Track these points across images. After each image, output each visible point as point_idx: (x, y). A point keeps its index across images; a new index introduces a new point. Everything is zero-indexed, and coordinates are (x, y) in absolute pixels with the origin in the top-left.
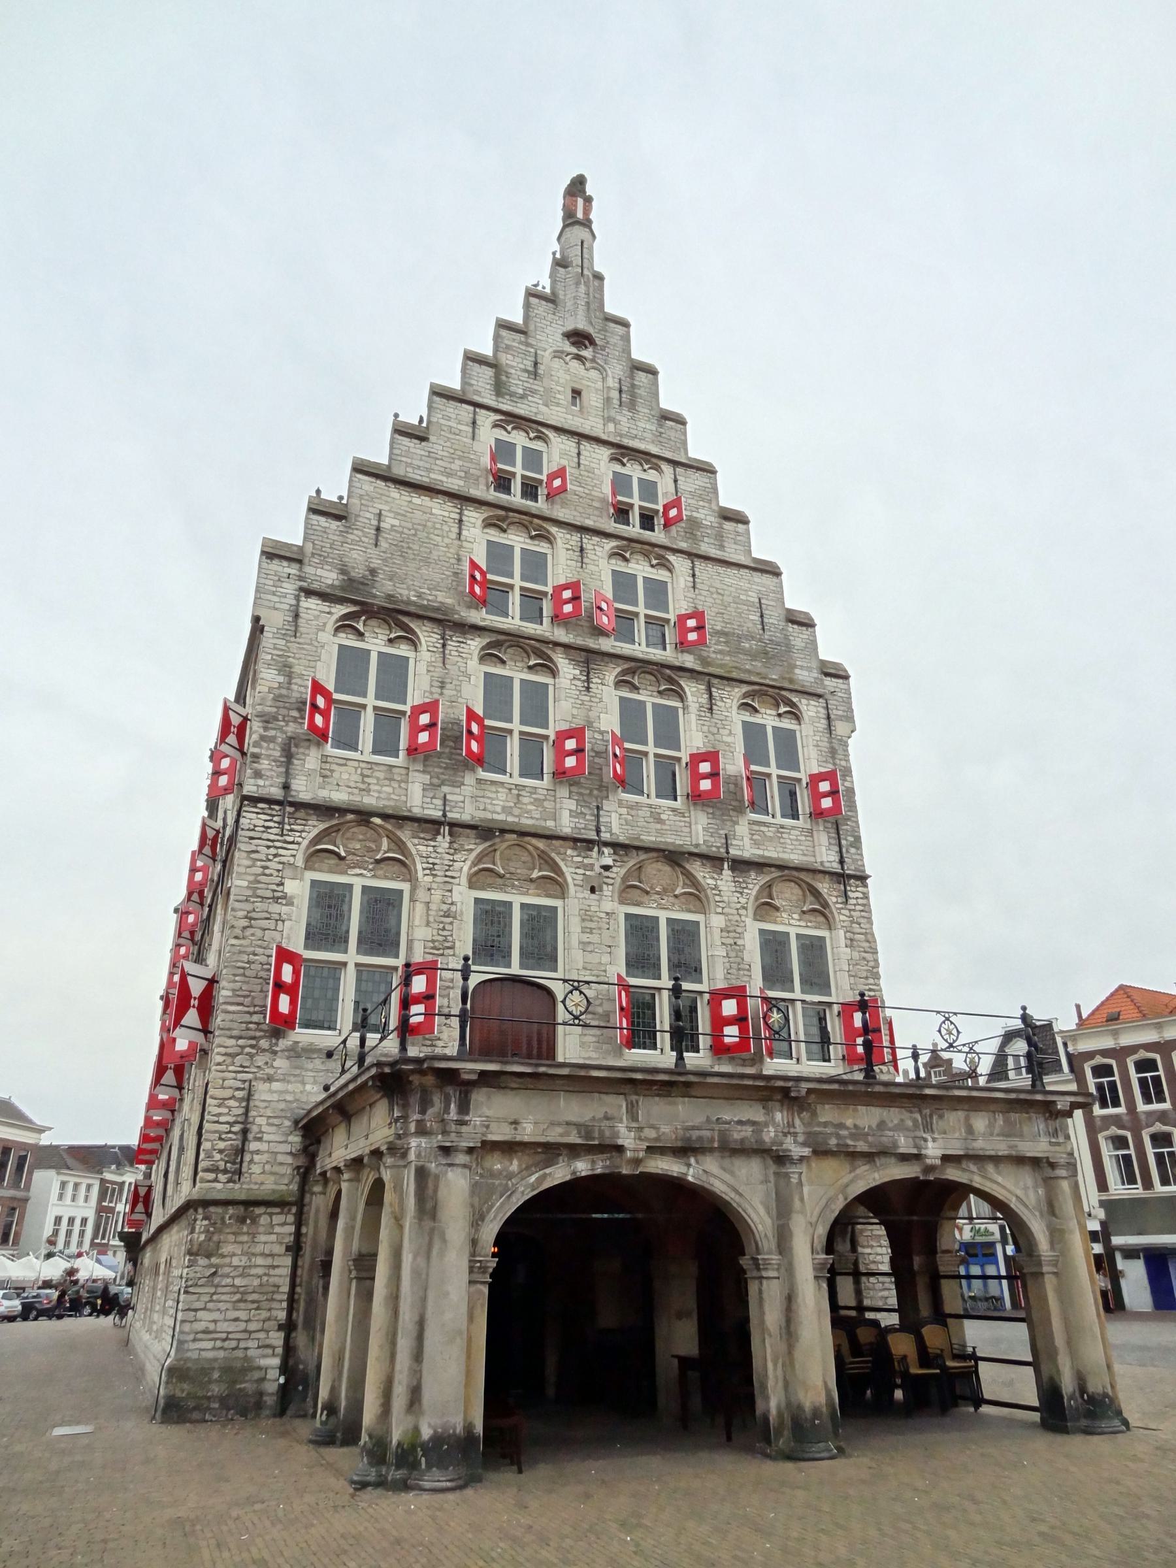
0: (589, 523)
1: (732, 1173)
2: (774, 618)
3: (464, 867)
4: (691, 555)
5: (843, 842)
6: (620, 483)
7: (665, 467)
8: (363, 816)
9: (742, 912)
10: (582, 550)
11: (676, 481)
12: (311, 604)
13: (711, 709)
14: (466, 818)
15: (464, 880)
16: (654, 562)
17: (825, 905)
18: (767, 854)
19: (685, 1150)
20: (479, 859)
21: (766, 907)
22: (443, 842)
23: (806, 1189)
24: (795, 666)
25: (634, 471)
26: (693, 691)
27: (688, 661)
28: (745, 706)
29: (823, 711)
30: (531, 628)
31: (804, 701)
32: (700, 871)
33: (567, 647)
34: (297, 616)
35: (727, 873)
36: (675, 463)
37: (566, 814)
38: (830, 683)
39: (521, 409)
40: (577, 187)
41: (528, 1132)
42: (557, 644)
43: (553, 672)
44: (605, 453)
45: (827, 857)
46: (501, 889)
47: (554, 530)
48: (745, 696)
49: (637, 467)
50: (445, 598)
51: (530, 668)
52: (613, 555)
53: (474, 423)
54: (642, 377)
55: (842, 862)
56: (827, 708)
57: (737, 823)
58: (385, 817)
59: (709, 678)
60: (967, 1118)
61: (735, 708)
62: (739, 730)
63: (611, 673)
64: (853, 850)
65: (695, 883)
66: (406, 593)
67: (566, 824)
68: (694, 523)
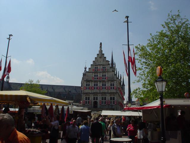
4: (108, 72)
6: (103, 68)
8: (88, 93)
12: (85, 82)
25: (104, 66)
30: (97, 80)
32: (106, 94)
36: (107, 65)
40: (101, 44)
43: (98, 83)
44: (102, 66)
50: (92, 79)
54: (105, 59)
59: (108, 81)
62: (110, 84)
66: (89, 80)
67: (98, 92)
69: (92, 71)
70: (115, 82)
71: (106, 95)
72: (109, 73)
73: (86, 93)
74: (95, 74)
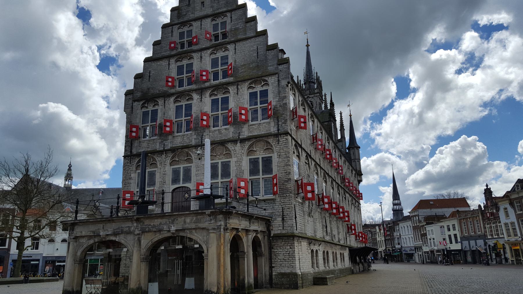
0: (204, 47)
1: (126, 239)
2: (262, 51)
3: (168, 161)
4: (235, 42)
5: (280, 123)
6: (215, 27)
7: (229, 14)
9: (243, 155)
10: (201, 57)
11: (231, 18)
12: (136, 104)
13: (238, 93)
14: (169, 148)
15: (168, 164)
16: (224, 50)
17: (272, 146)
18: (254, 134)
19: (115, 234)
20: (173, 157)
21: (250, 152)
22: (164, 156)
23: (142, 241)
24: (268, 66)
25: (219, 21)
26: (232, 89)
27: (231, 79)
28: (250, 88)
29: (276, 79)
31: (270, 78)
32: (230, 146)
33: (195, 90)
34: (132, 108)
35: (239, 144)
36: (231, 11)
37: (193, 140)
38: (280, 67)
39: (185, 19)
41: (84, 234)
42: (193, 91)
43: (192, 99)
44: (209, 20)
45: (273, 130)
46: (178, 164)
47: (193, 54)
48: (250, 84)
49: (220, 19)
50: (165, 89)
51: (187, 100)
52: (211, 54)
53: (172, 31)
55: (278, 130)
56: (279, 77)
57: (243, 128)
58: (151, 153)
59: (237, 83)
60: (185, 219)
61: (246, 89)
62: (247, 97)
63: (208, 94)
64: (283, 125)
65: (229, 150)
67: (193, 143)
68: (236, 29)
69: (168, 53)
70: (272, 80)
71: (227, 149)
72: (239, 45)
73: (138, 155)
74: (179, 64)
